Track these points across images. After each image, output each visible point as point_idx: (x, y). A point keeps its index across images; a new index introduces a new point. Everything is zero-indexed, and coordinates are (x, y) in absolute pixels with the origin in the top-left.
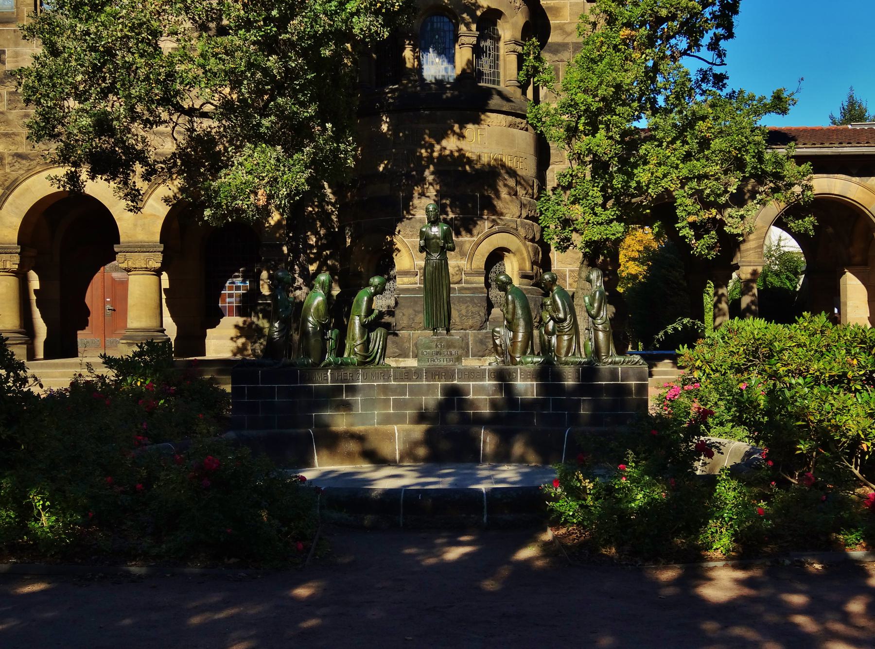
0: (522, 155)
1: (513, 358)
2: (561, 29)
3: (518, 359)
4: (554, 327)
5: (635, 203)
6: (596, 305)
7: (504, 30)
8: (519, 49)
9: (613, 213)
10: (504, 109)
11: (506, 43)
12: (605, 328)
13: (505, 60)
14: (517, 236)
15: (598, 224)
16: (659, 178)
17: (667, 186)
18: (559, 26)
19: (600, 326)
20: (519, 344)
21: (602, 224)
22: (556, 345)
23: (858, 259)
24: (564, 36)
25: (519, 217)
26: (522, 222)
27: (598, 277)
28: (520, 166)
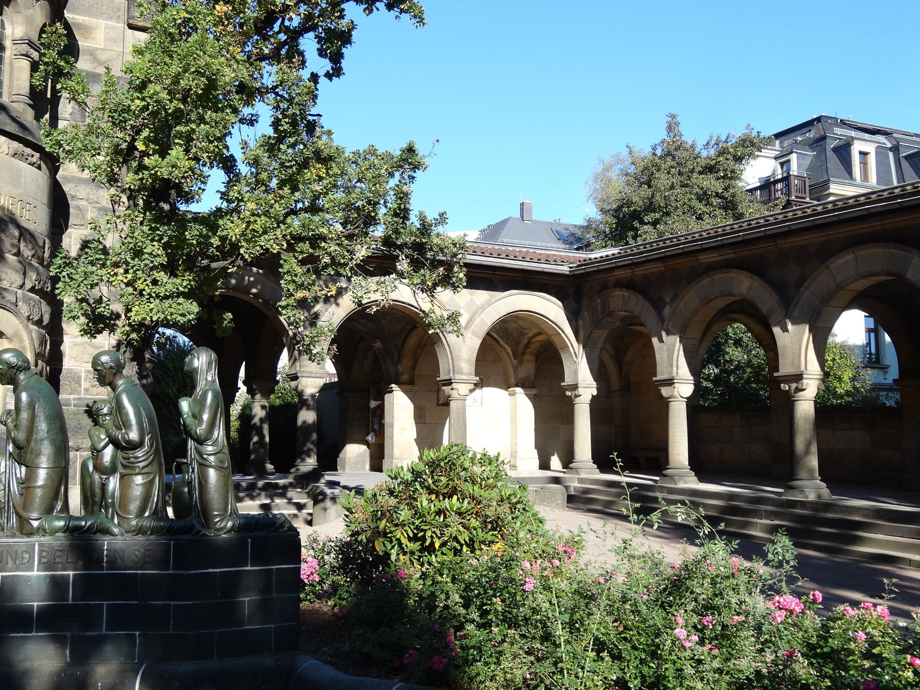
0: (30, 200)
1: (23, 522)
2: (91, 55)
3: (35, 524)
4: (114, 458)
5: (215, 269)
6: (206, 417)
7: (13, 24)
8: (35, 55)
9: (185, 284)
10: (7, 129)
11: (15, 42)
12: (222, 461)
13: (11, 65)
14: (16, 314)
15: (158, 296)
16: (257, 232)
17: (268, 246)
18: (89, 51)
19: (212, 458)
20: (39, 492)
21: (166, 297)
22: (117, 494)
23: (405, 377)
24: (95, 64)
25: (21, 287)
26: (24, 296)
27: (210, 364)
28: (26, 215)
